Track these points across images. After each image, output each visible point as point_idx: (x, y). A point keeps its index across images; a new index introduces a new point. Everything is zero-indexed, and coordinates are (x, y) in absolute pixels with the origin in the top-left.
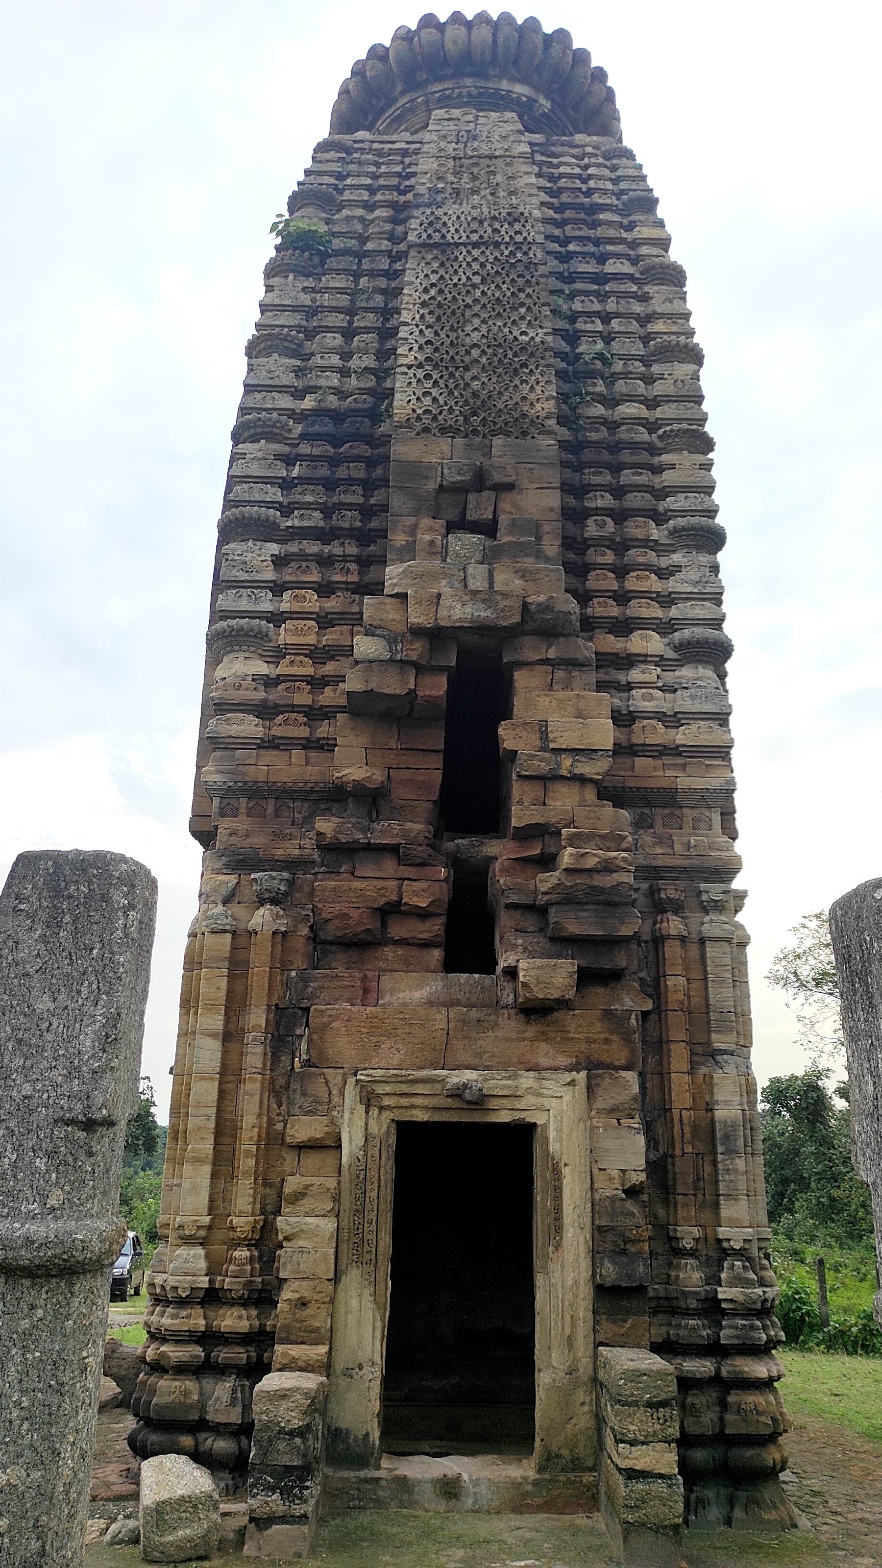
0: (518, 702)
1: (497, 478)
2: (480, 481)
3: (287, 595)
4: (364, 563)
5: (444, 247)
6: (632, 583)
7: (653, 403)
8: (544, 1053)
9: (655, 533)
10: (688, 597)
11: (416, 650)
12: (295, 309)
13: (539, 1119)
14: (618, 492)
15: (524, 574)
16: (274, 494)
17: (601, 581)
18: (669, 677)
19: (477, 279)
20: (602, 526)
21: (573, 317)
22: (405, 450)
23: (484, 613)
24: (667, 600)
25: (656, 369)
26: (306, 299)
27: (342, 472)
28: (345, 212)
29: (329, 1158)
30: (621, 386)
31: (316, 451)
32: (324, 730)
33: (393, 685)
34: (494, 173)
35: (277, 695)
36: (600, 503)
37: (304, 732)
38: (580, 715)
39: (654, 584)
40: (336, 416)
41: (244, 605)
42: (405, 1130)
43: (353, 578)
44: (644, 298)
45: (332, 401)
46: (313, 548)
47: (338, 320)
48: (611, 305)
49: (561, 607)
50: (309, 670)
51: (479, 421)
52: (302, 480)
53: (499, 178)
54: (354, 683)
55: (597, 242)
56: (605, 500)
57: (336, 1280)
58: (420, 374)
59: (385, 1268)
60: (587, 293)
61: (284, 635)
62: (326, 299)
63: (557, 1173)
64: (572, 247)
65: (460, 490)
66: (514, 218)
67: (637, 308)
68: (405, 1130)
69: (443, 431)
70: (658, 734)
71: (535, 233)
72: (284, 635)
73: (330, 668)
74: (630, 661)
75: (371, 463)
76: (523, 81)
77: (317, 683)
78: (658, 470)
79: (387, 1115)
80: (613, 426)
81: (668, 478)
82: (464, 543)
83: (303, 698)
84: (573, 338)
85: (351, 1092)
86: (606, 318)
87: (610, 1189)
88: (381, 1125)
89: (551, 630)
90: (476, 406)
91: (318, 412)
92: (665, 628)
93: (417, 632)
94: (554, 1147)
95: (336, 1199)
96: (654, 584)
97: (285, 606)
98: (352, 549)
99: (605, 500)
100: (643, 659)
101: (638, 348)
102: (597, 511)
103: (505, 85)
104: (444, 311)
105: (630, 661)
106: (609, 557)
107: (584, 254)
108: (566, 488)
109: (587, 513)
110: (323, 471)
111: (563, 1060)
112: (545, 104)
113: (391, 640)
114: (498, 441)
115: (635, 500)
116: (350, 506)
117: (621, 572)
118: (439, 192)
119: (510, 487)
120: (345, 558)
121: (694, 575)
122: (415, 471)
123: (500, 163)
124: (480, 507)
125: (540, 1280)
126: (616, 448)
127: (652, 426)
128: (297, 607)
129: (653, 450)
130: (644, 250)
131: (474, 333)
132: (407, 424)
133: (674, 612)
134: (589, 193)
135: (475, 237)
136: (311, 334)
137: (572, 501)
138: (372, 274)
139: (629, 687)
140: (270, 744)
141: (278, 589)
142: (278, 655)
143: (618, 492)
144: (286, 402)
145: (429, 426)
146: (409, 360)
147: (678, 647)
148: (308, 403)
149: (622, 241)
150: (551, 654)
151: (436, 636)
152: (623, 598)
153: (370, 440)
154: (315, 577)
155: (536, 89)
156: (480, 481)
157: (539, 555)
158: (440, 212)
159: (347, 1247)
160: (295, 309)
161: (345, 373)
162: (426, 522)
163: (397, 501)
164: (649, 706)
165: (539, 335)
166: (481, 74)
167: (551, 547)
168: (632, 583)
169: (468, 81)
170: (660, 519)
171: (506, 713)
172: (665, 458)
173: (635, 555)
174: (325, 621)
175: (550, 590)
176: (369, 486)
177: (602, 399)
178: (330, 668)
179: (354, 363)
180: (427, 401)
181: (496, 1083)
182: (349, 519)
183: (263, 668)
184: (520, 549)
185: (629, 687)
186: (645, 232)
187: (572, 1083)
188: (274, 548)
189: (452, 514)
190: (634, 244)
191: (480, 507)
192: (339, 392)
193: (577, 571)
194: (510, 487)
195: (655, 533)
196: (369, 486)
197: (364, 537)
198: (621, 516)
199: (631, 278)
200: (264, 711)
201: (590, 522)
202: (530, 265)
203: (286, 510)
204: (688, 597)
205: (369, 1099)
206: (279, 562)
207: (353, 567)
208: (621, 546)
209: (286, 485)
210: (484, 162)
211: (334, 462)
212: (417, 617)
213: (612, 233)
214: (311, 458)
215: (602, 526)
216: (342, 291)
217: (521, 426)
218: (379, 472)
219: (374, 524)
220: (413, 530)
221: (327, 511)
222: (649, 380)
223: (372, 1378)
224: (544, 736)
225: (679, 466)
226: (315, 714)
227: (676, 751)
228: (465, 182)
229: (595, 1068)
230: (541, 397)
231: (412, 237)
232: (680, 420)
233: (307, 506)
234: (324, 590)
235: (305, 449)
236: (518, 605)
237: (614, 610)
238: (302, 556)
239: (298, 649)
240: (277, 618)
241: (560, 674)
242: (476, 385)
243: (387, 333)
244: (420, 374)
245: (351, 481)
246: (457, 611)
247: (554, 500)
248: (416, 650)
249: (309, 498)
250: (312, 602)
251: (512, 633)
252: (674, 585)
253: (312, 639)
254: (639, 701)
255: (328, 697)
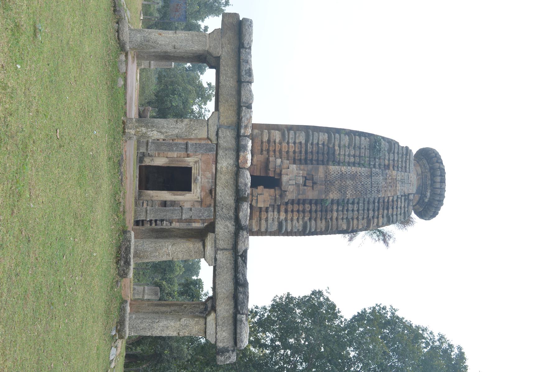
0: (267, 190)
1: (315, 186)
2: (314, 183)
3: (293, 145)
4: (300, 160)
5: (371, 176)
6: (295, 213)
7: (337, 219)
8: (203, 194)
9: (306, 219)
10: (292, 224)
11: (278, 171)
12: (360, 144)
13: (192, 192)
14: (316, 211)
15: (293, 191)
16: (315, 142)
17: (296, 207)
18: (276, 220)
19: (363, 183)
20: (308, 208)
21: (358, 203)
22: (321, 168)
23: (284, 184)
24: (292, 220)
25: (345, 220)
26: (363, 146)
27: (320, 155)
28: (387, 154)
29: (186, 156)
30: (341, 213)
31: (325, 150)
32: (265, 153)
33: (271, 166)
34: (391, 187)
35: (272, 144)
36: (313, 207)
37: (264, 149)
38: (264, 201)
39: (295, 218)
40: (334, 154)
41: (291, 136)
42: (191, 168)
43: (296, 158)
44: (363, 219)
45: (337, 152)
46: (303, 150)
47: (357, 153)
48: (361, 212)
49: (286, 198)
50: (277, 150)
51: (328, 183)
52: (318, 147)
53: (390, 188)
54: (271, 159)
55: (378, 209)
56: (314, 208)
57: (167, 157)
58: (339, 171)
59: (168, 165)
60: (364, 207)
61: (284, 144)
62: (363, 151)
63: (183, 195)
64: (376, 204)
65: (313, 179)
66: (378, 191)
67: (360, 217)
68: (190, 169)
69: (326, 176)
70: (264, 216)
71: (374, 195)
72: (284, 144)
73: (277, 153)
74: (279, 212)
75: (323, 161)
76: (431, 195)
77: (274, 151)
78: (321, 219)
79: (193, 166)
80: (332, 211)
81: (319, 221)
82: (301, 181)
83: (271, 148)
84: (353, 203)
85: (196, 159)
86: (358, 210)
87: (181, 204)
88: (191, 165)
89: (281, 196)
90: (332, 183)
91: (334, 150)
92: (286, 220)
93: (281, 171)
94: (188, 195)
95: (180, 157)
96: (295, 218)
97: (290, 144)
98: (303, 158)
99: (314, 208)
100: (279, 215)
101: (350, 217)
102: (311, 207)
103: (429, 191)
104: (354, 177)
105: (279, 212)
106: (301, 209)
107: (374, 207)
108: (317, 200)
109: (311, 205)
110: (320, 151)
111: (202, 196)
112: (426, 200)
113: (280, 166)
114: (324, 187)
115: (314, 215)
116: (312, 157)
117: (298, 211)
118: (386, 175)
119: (313, 189)
120: (301, 156)
121: (297, 225)
122: (317, 170)
123: (395, 188)
124: (309, 183)
125: (166, 192)
126: (326, 211)
127: (331, 219)
128: (290, 147)
129: (326, 219)
130: (376, 220)
131: (349, 182)
132: (327, 169)
133: (289, 222)
134: (393, 208)
135: (373, 183)
136: (354, 148)
137: (313, 202)
138: (370, 161)
139: (273, 212)
140: (262, 142)
141: (295, 143)
142: (280, 143)
143: (316, 211)
144: (337, 143)
145: (327, 173)
146: (342, 169)
147: (281, 222)
148: (337, 148)
149: (378, 215)
150: (277, 196)
151: (280, 174)
152: (292, 211)
153: (328, 161)
154: (297, 150)
155: (429, 198)
156: (314, 183)
157: (299, 194)
158: (380, 175)
159: (172, 159)
160: (360, 144)
161: (345, 155)
162: (305, 172)
163: (310, 167)
164: (269, 215)
165: (348, 196)
166: (432, 185)
167: (300, 197)
168: (295, 213)
169: (430, 182)
170: (310, 219)
171: (265, 187)
172: (324, 221)
173: (301, 215)
174: (288, 152)
175: (290, 196)
176: (317, 160)
177: (338, 209)
178: (277, 153)
179: (347, 157)
180: (333, 173)
181: (199, 185)
182: (310, 156)
183: (277, 141)
184: (299, 190)
185: (273, 212)
186: (381, 220)
187: (198, 198)
188: (303, 142)
189: (308, 178)
190: (378, 218)
191: (309, 183)
192: (339, 154)
193: (293, 202)
194: (313, 189)
195: (306, 219)
196: (317, 160)
197: (306, 159)
198: (310, 212)
199: (368, 217)
200: (269, 141)
201: (309, 205)
202: (366, 194)
203: (312, 144)
204: (292, 224)
205: (196, 162)
206: (300, 143)
207: (299, 158)
208: (304, 211)
209: (318, 144)
210: (395, 185)
211: (323, 154)
212: (283, 171)
213: (380, 213)
214: (324, 149)
215: (308, 208)
216: (365, 155)
217: (327, 192)
218: (320, 162)
219: (308, 162)
220: (303, 170)
221: (312, 152)
222: (343, 219)
223: (152, 164)
224: (261, 194)
225: (322, 225)
226: (268, 151)
227: (260, 220)
228: (389, 181)
229: (201, 202)
230: (334, 195)
231: (373, 169)
232: (332, 225)
233: (313, 148)
234: (294, 152)
235: (326, 148)
236: (286, 190)
237: (290, 209)
238: (301, 147)
239: (281, 147)
240: (288, 143)
241: (273, 198)
242: (337, 182)
243: (354, 164)
244: (339, 171)
245: (318, 157)
246: (285, 179)
247: (310, 198)
248: (278, 171)
249: (314, 149)
250: (291, 150)
251: (281, 189)
252: (295, 222)
253: (283, 150)
254: (270, 214)
255: (271, 153)
